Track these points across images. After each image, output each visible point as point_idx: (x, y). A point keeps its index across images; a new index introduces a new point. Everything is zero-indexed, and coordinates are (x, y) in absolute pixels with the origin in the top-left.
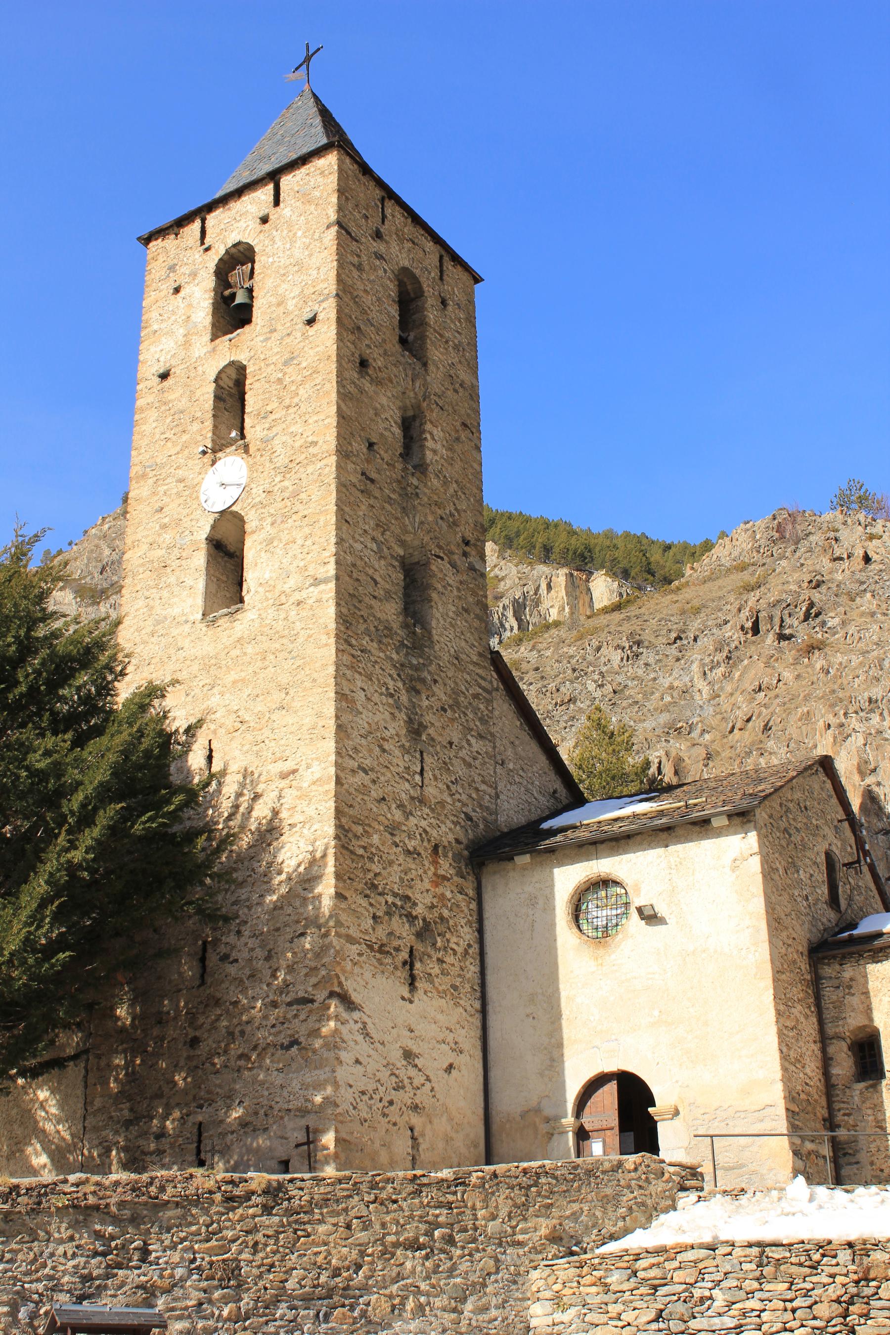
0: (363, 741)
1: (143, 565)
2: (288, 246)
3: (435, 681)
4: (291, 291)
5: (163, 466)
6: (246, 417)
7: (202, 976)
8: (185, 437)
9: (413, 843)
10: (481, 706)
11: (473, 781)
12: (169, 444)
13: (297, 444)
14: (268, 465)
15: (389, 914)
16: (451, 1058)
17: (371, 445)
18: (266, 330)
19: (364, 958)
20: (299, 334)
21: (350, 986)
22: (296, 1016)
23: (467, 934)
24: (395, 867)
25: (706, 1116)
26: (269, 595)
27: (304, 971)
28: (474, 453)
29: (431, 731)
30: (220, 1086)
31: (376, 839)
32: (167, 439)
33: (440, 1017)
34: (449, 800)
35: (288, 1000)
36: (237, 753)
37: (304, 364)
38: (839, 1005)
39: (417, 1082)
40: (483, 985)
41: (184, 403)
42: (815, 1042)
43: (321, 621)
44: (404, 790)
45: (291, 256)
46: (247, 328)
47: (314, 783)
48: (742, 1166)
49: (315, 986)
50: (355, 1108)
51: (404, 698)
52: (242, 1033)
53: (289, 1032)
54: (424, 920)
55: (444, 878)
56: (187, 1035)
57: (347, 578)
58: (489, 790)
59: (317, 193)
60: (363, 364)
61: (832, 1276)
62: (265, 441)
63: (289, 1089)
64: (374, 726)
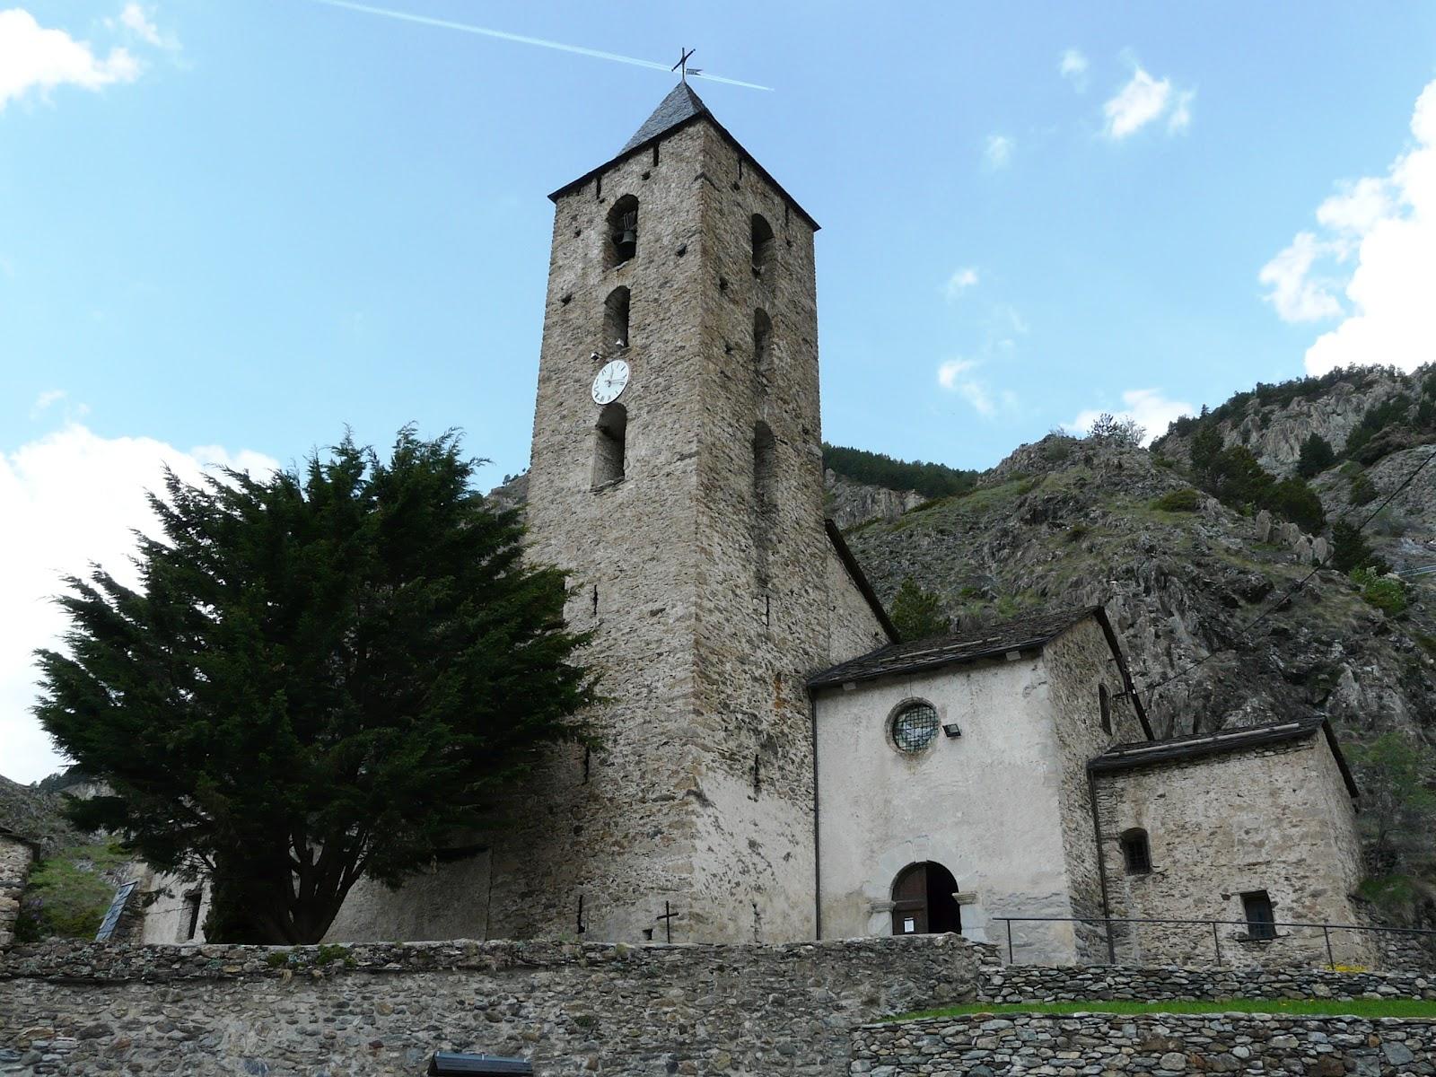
0: (720, 588)
1: (547, 448)
3: (780, 542)
4: (666, 230)
5: (564, 370)
6: (629, 329)
7: (586, 776)
8: (581, 347)
9: (760, 671)
10: (818, 564)
11: (810, 623)
12: (569, 353)
13: (670, 349)
15: (739, 728)
16: (789, 848)
17: (728, 350)
18: (646, 261)
19: (717, 764)
20: (672, 263)
21: (705, 786)
22: (660, 811)
23: (803, 747)
24: (744, 690)
26: (644, 469)
27: (667, 773)
28: (813, 361)
29: (775, 581)
30: (598, 868)
31: (728, 667)
32: (567, 350)
33: (780, 815)
34: (790, 638)
35: (654, 797)
36: (617, 596)
37: (675, 287)
38: (1111, 811)
39: (760, 868)
40: (816, 789)
41: (581, 321)
42: (1092, 841)
43: (686, 488)
44: (753, 629)
45: (665, 203)
46: (632, 261)
47: (678, 620)
48: (1031, 945)
49: (675, 786)
50: (707, 888)
51: (754, 553)
52: (616, 824)
53: (654, 823)
54: (768, 735)
55: (785, 700)
56: (571, 825)
57: (707, 455)
58: (823, 631)
59: (688, 154)
60: (723, 285)
61: (1119, 1047)
62: (645, 347)
64: (728, 577)
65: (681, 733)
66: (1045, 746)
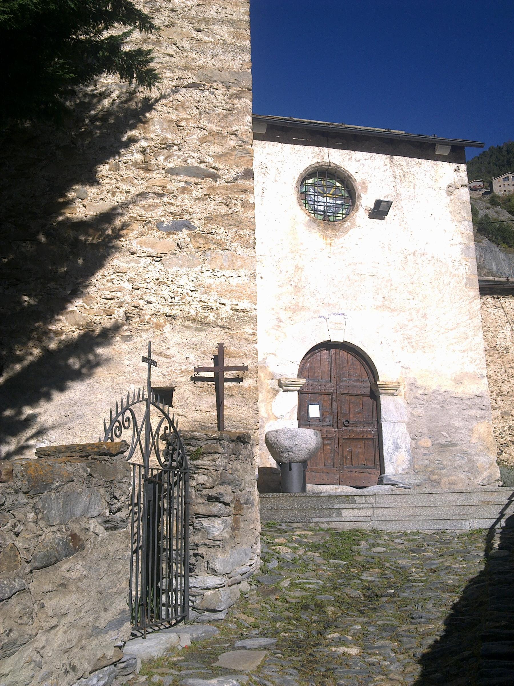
25: (425, 397)
63: (174, 288)
65: (226, 76)
66: (468, 248)
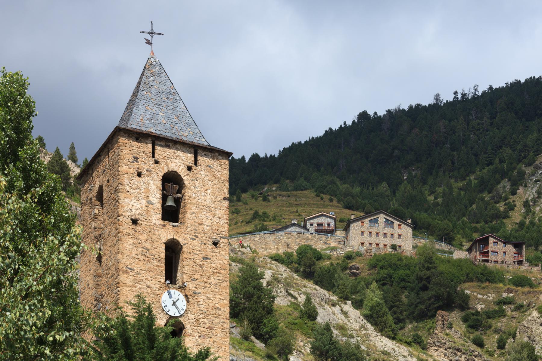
2: (203, 194)
13: (211, 305)
14: (196, 306)
37: (213, 265)
